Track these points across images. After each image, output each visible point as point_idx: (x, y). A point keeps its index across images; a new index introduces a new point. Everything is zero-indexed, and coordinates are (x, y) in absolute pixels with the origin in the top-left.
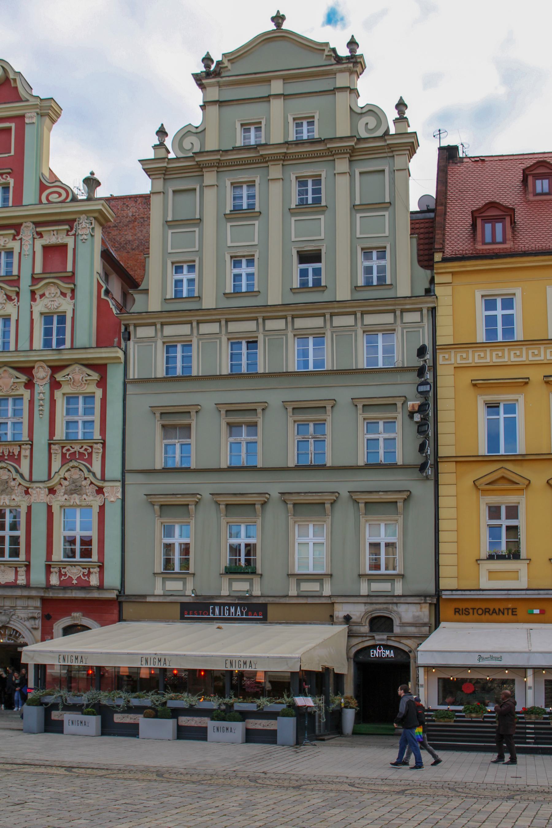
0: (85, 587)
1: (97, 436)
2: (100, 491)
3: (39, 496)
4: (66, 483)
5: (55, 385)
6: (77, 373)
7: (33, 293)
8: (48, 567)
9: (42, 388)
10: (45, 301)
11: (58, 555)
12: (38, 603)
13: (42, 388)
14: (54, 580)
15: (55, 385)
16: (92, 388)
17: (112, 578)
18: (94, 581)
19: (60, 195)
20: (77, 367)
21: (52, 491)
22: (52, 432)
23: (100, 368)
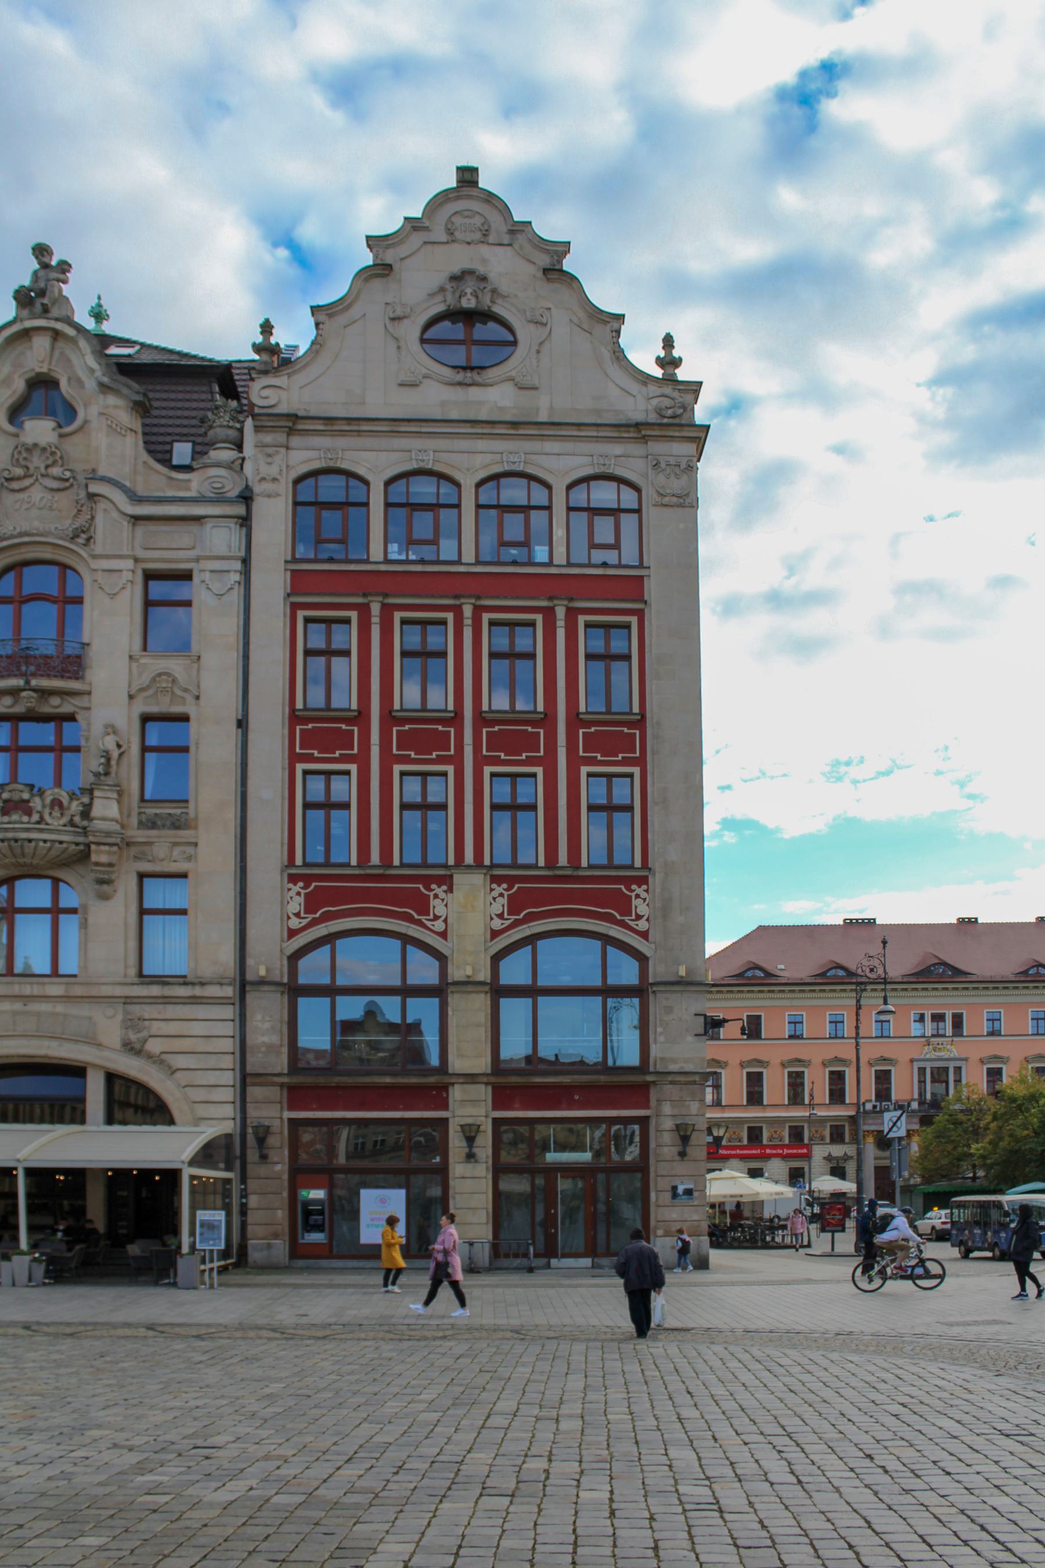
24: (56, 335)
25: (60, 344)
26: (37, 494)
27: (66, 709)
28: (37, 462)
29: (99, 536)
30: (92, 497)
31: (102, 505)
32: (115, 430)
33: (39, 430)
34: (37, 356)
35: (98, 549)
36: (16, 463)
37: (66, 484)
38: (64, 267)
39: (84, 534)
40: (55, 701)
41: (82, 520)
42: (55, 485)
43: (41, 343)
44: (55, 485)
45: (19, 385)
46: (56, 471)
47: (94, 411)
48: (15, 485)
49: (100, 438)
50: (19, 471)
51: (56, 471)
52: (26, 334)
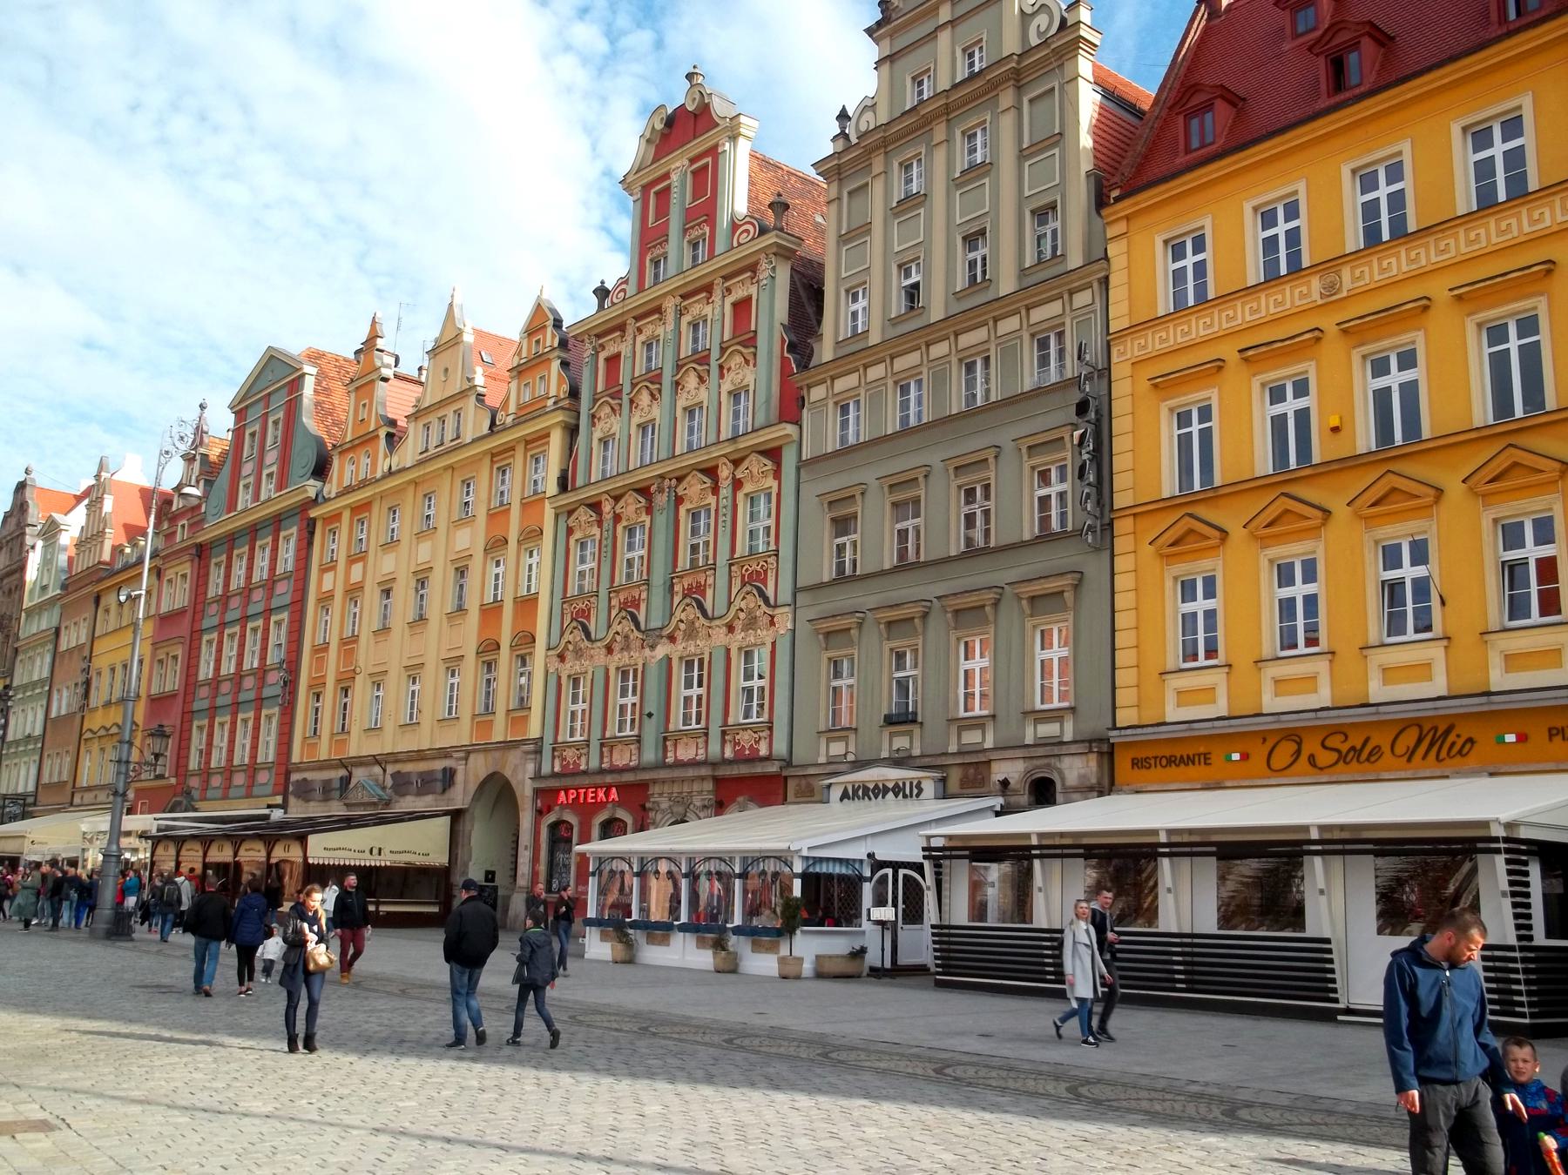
0: (754, 759)
1: (773, 547)
2: (772, 623)
3: (720, 636)
4: (742, 616)
5: (737, 484)
6: (757, 464)
7: (721, 367)
8: (724, 733)
9: (725, 491)
10: (732, 374)
11: (737, 716)
12: (709, 786)
13: (725, 491)
14: (729, 754)
16: (771, 482)
17: (780, 747)
18: (763, 751)
19: (747, 231)
20: (754, 457)
21: (731, 628)
22: (733, 550)
23: (773, 454)
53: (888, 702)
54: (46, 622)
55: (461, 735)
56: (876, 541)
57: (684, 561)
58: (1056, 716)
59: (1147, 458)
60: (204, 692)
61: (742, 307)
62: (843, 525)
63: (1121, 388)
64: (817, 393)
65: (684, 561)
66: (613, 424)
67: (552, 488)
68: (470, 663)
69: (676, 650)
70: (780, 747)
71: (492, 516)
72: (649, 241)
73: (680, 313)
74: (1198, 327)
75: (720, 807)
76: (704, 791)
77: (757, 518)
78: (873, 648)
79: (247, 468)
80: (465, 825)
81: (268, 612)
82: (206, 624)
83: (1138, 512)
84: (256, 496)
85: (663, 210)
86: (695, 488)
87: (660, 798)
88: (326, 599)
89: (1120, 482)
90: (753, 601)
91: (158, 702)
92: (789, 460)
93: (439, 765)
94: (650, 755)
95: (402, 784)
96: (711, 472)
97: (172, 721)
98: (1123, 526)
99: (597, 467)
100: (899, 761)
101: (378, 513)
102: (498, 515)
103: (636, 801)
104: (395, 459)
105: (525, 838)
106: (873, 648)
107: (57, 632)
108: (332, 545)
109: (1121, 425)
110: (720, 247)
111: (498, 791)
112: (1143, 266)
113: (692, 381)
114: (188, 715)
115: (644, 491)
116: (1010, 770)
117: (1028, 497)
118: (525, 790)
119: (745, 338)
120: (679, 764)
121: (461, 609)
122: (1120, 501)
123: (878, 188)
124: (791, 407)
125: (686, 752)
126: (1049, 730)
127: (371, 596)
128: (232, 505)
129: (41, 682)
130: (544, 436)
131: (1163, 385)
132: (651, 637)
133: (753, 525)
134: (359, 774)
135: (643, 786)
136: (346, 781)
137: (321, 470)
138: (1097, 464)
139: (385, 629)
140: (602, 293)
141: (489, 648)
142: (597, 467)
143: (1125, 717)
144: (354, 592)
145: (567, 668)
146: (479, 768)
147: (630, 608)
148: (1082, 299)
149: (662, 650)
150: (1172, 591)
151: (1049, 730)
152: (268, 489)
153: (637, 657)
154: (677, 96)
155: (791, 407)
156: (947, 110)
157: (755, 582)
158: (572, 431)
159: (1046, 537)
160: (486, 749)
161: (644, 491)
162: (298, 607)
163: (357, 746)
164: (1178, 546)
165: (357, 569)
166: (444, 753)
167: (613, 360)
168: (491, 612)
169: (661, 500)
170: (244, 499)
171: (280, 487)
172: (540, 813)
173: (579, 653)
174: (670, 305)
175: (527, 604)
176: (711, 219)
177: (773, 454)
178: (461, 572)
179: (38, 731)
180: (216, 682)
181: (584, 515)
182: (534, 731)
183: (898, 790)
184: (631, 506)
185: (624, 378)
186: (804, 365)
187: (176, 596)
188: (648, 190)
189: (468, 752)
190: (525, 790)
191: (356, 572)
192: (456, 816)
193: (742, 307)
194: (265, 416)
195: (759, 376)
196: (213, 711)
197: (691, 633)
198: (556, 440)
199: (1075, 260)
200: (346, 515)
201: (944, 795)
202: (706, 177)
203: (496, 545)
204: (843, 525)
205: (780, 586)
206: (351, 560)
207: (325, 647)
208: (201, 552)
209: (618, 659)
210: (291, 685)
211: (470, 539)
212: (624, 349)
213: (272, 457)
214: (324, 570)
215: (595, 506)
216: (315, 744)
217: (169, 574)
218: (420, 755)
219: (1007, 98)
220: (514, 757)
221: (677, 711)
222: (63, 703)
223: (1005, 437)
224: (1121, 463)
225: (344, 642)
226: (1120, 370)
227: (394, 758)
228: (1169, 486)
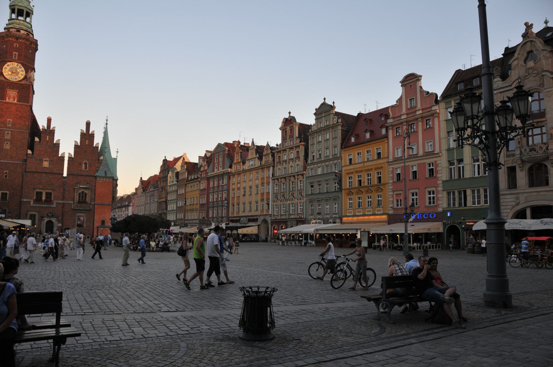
0: (301, 218)
3: (296, 200)
5: (298, 179)
6: (300, 177)
15: (298, 179)
17: (305, 217)
23: (302, 175)
24: (532, 41)
25: (533, 43)
26: (531, 78)
27: (542, 125)
28: (530, 71)
29: (545, 84)
30: (543, 75)
31: (545, 77)
32: (546, 58)
33: (531, 64)
34: (528, 47)
35: (545, 87)
36: (526, 72)
37: (537, 74)
38: (532, 25)
39: (542, 85)
40: (540, 124)
41: (541, 82)
42: (535, 75)
43: (529, 44)
44: (535, 75)
45: (525, 55)
46: (535, 72)
47: (541, 55)
48: (527, 77)
49: (544, 62)
50: (527, 74)
51: (535, 72)
52: (525, 43)
53: (318, 212)
54: (174, 188)
55: (259, 213)
56: (316, 189)
57: (291, 190)
58: (336, 214)
59: (346, 184)
60: (211, 204)
61: (298, 152)
62: (312, 186)
63: (343, 173)
64: (308, 167)
65: (291, 190)
66: (279, 167)
67: (271, 176)
68: (259, 202)
69: (291, 202)
70: (305, 217)
71: (262, 179)
72: (284, 139)
73: (289, 151)
74: (351, 167)
75: (297, 225)
76: (295, 223)
77: (301, 184)
78: (316, 204)
79: (216, 165)
80: (260, 227)
81: (223, 191)
82: (211, 192)
83: (345, 190)
84: (218, 170)
85: (286, 134)
86: (292, 178)
87: (289, 223)
88: (233, 189)
89: (343, 185)
90: (300, 196)
91: (202, 205)
92: (305, 176)
93: (255, 218)
94: (287, 217)
95: (250, 221)
96: (294, 176)
97: (206, 208)
98: (343, 191)
99: (278, 174)
100: (319, 219)
101: (242, 175)
102: (263, 179)
103: (285, 223)
104: (244, 167)
105: (270, 229)
106: (316, 204)
107: (177, 191)
108: (234, 180)
109: (343, 178)
110: (295, 143)
111: (265, 221)
112: (346, 156)
113: (291, 162)
114: (208, 208)
115: (285, 178)
116: (331, 221)
117: (333, 186)
118: (269, 222)
119: (298, 158)
120: (291, 219)
121: (257, 193)
122: (343, 188)
123: (315, 139)
124: (305, 169)
125: (292, 217)
126: (335, 216)
127: (242, 190)
128: (213, 171)
129: (175, 200)
130: (269, 167)
131: (348, 174)
132: (287, 200)
133: (300, 185)
134: (242, 219)
135: (286, 221)
136: (240, 220)
137: (231, 167)
138: (340, 183)
139: (244, 195)
140: (277, 145)
141: (262, 200)
142: (278, 174)
143: (343, 215)
144: (239, 189)
145: (275, 203)
146: (262, 218)
147: (283, 196)
148: (339, 160)
149: (288, 202)
150: (348, 200)
151: (335, 216)
152: (221, 170)
153: (285, 202)
154: (287, 117)
155: (305, 169)
156: (324, 130)
157: (301, 194)
158: (274, 166)
159: (335, 191)
160: (263, 215)
161: (285, 178)
162: (228, 190)
163: (241, 214)
164: (348, 194)
165: (239, 185)
166: (256, 216)
167: (279, 156)
168: (262, 194)
169: (287, 180)
170: (216, 170)
171: (223, 169)
172: (272, 225)
173: (276, 202)
174: (288, 150)
175: (268, 193)
176: (293, 138)
177: (302, 175)
178: (257, 187)
179: (175, 209)
180: (213, 202)
181: (276, 181)
182: (270, 213)
183: (319, 223)
184: (283, 180)
185: (281, 160)
186: (307, 162)
187: (203, 185)
188: (283, 129)
189: (260, 215)
190: (269, 222)
191: (239, 185)
192: (258, 225)
193: (298, 152)
194: (219, 156)
195: (301, 162)
196: (213, 207)
197: (292, 200)
198: (271, 169)
199: (339, 155)
200: (236, 175)
201: (324, 223)
202: (292, 130)
203: (263, 184)
204: (312, 186)
205: (304, 194)
206: (238, 183)
207: (234, 197)
208: (208, 179)
209: (282, 203)
210: (228, 203)
211: (258, 182)
212: (281, 155)
213: (221, 163)
214: (233, 184)
215: (278, 179)
216: (234, 213)
217: (202, 182)
218: (252, 216)
219: (331, 130)
220: (267, 217)
221: (291, 211)
222: (180, 204)
223: (330, 178)
224: (343, 183)
225: (237, 197)
226: (343, 171)
227: (248, 216)
228: (348, 187)
